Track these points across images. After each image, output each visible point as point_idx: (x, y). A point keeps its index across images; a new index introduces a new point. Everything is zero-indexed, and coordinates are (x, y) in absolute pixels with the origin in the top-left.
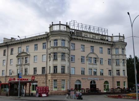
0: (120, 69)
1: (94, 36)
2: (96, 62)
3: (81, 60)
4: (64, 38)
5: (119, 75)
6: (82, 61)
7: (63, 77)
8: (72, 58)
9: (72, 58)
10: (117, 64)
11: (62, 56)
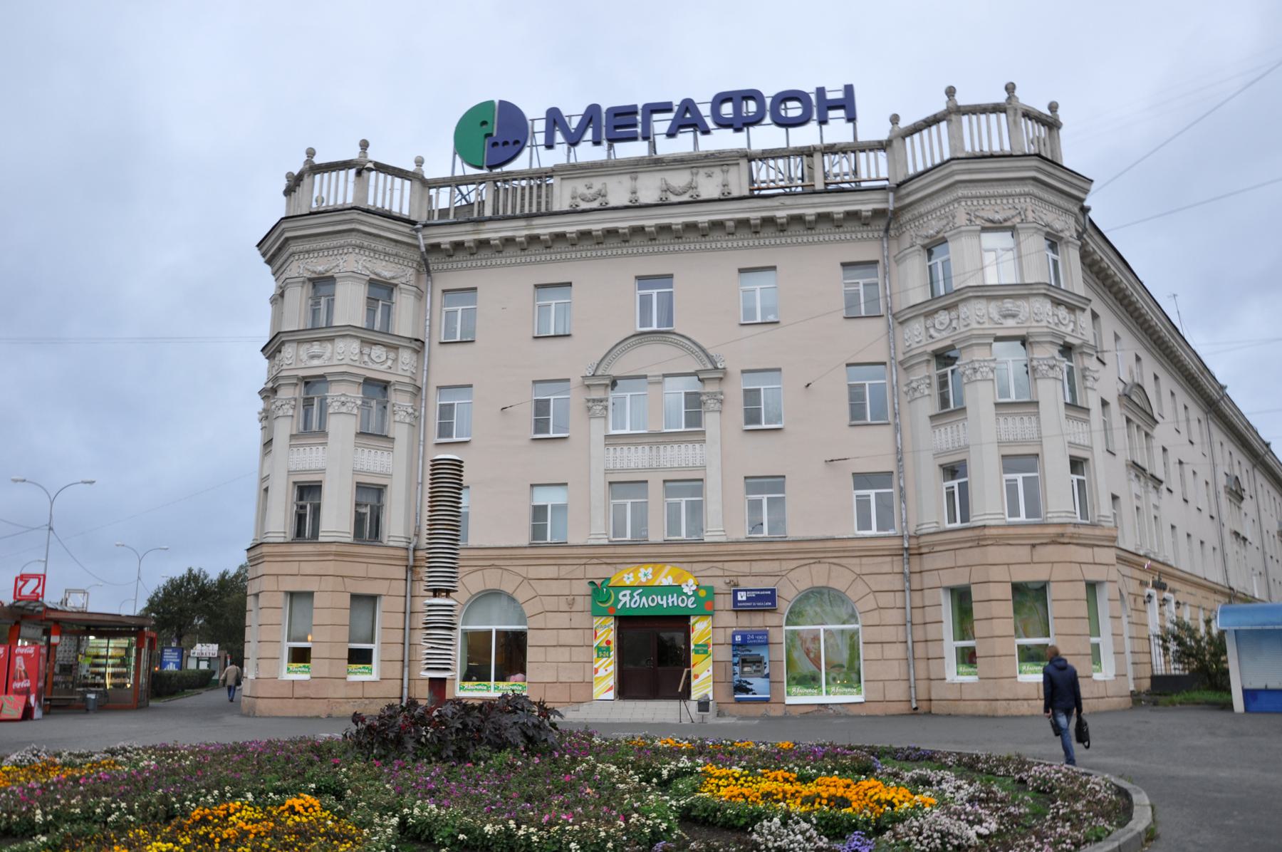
0: (966, 448)
1: (679, 179)
2: (694, 418)
3: (527, 414)
4: (320, 265)
5: (965, 518)
6: (541, 425)
7: (292, 568)
8: (446, 411)
9: (446, 411)
10: (944, 402)
11: (308, 403)
